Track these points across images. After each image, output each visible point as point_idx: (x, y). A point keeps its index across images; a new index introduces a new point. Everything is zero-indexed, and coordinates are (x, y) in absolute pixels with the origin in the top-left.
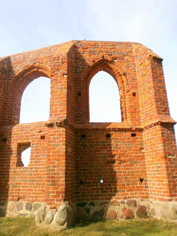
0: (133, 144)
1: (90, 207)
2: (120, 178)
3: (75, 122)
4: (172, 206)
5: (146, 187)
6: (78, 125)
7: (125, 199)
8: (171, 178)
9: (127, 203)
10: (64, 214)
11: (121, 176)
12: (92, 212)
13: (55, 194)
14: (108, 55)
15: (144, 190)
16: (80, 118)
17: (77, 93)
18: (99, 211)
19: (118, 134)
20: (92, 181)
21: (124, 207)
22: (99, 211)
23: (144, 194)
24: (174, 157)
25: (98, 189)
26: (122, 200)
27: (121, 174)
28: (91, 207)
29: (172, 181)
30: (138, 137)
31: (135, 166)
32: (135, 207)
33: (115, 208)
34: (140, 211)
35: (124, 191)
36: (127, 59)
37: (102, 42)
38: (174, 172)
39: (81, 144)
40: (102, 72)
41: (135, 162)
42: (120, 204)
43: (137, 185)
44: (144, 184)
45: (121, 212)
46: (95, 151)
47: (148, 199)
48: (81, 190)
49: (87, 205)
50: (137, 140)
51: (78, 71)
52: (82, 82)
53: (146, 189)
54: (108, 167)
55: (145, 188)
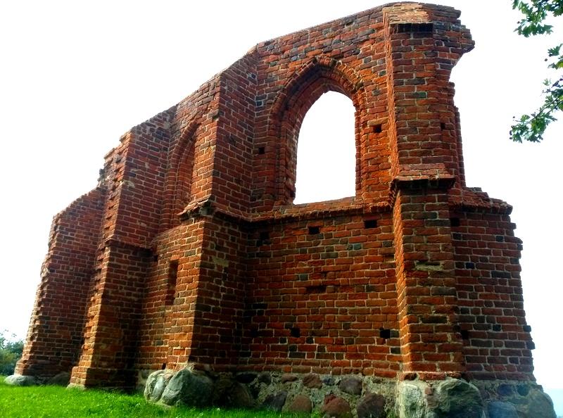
0: (367, 244)
1: (259, 386)
2: (334, 325)
3: (251, 209)
4: (407, 390)
5: (393, 351)
6: (256, 214)
7: (336, 374)
8: (420, 323)
9: (338, 384)
10: (179, 383)
11: (336, 322)
12: (263, 395)
13: (179, 348)
14: (325, 53)
15: (389, 357)
16: (260, 200)
17: (257, 149)
18: (275, 395)
19: (334, 225)
20: (274, 330)
21: (332, 393)
22: (275, 395)
23: (386, 367)
24: (439, 268)
25: (285, 349)
26: (330, 376)
27: (336, 315)
28: (263, 385)
29: (421, 330)
30: (381, 227)
31: (369, 299)
32: (356, 394)
33: (310, 392)
34: (367, 407)
35: (340, 357)
36: (367, 49)
37: (312, 29)
38: (432, 307)
39: (258, 252)
40: (330, 93)
41: (369, 289)
42: (323, 384)
43: (373, 345)
44: (389, 344)
45: (322, 403)
46: (285, 266)
47: (392, 380)
48: (251, 350)
49: (256, 380)
50: (377, 235)
51: (262, 105)
52: (267, 125)
53: (394, 355)
54: (309, 301)
55: (391, 354)
